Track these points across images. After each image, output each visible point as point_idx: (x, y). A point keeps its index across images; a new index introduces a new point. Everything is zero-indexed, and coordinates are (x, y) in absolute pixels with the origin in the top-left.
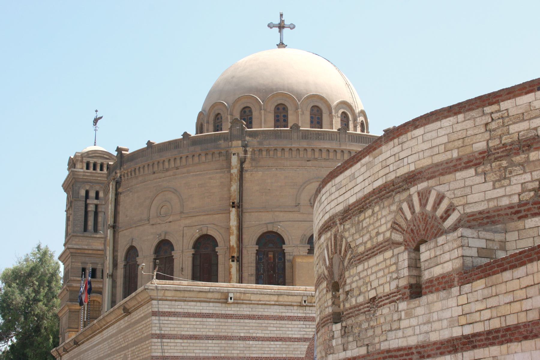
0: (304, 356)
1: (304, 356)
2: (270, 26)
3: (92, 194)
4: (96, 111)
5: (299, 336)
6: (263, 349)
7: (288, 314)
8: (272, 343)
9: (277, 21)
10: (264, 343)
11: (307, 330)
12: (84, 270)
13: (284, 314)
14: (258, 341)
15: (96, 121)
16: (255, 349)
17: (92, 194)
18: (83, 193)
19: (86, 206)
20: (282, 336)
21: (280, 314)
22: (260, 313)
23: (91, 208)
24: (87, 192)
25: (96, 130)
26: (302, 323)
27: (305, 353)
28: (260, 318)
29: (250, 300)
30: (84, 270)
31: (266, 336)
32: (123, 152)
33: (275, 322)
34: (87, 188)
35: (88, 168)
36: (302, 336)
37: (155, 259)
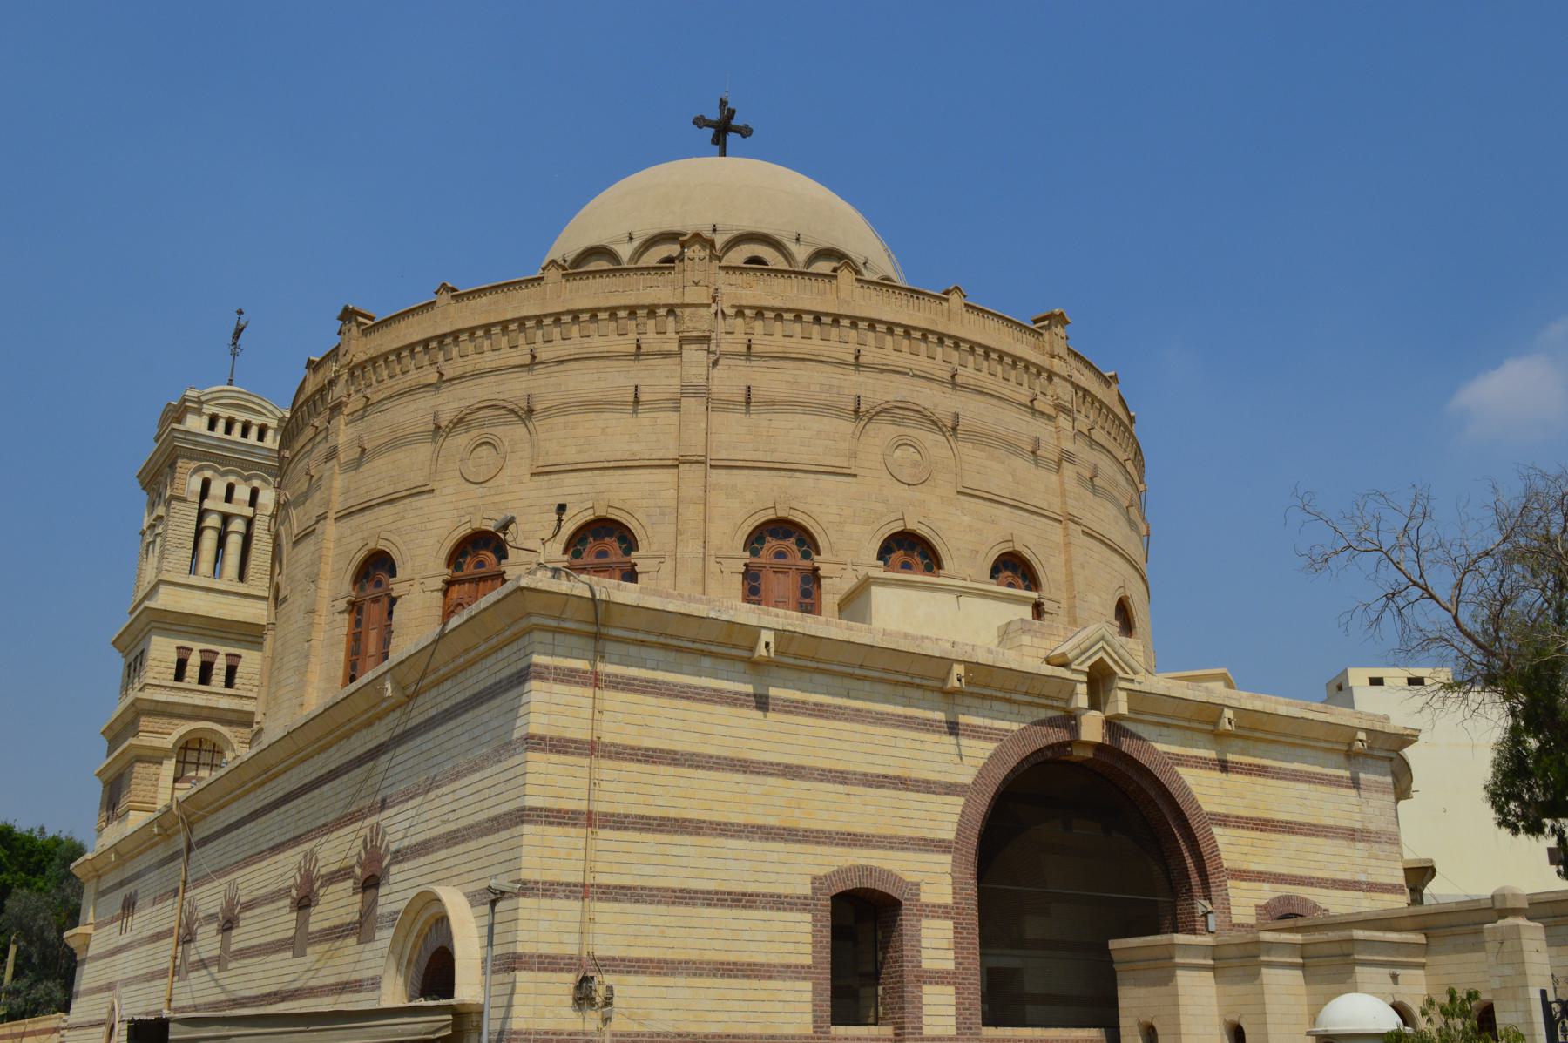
2: (700, 122)
3: (218, 488)
4: (240, 313)
9: (714, 115)
12: (181, 665)
15: (239, 332)
17: (218, 488)
18: (196, 484)
19: (202, 514)
23: (213, 521)
24: (206, 484)
25: (235, 355)
29: (812, 659)
30: (181, 665)
32: (360, 319)
34: (208, 474)
35: (212, 427)
37: (449, 584)
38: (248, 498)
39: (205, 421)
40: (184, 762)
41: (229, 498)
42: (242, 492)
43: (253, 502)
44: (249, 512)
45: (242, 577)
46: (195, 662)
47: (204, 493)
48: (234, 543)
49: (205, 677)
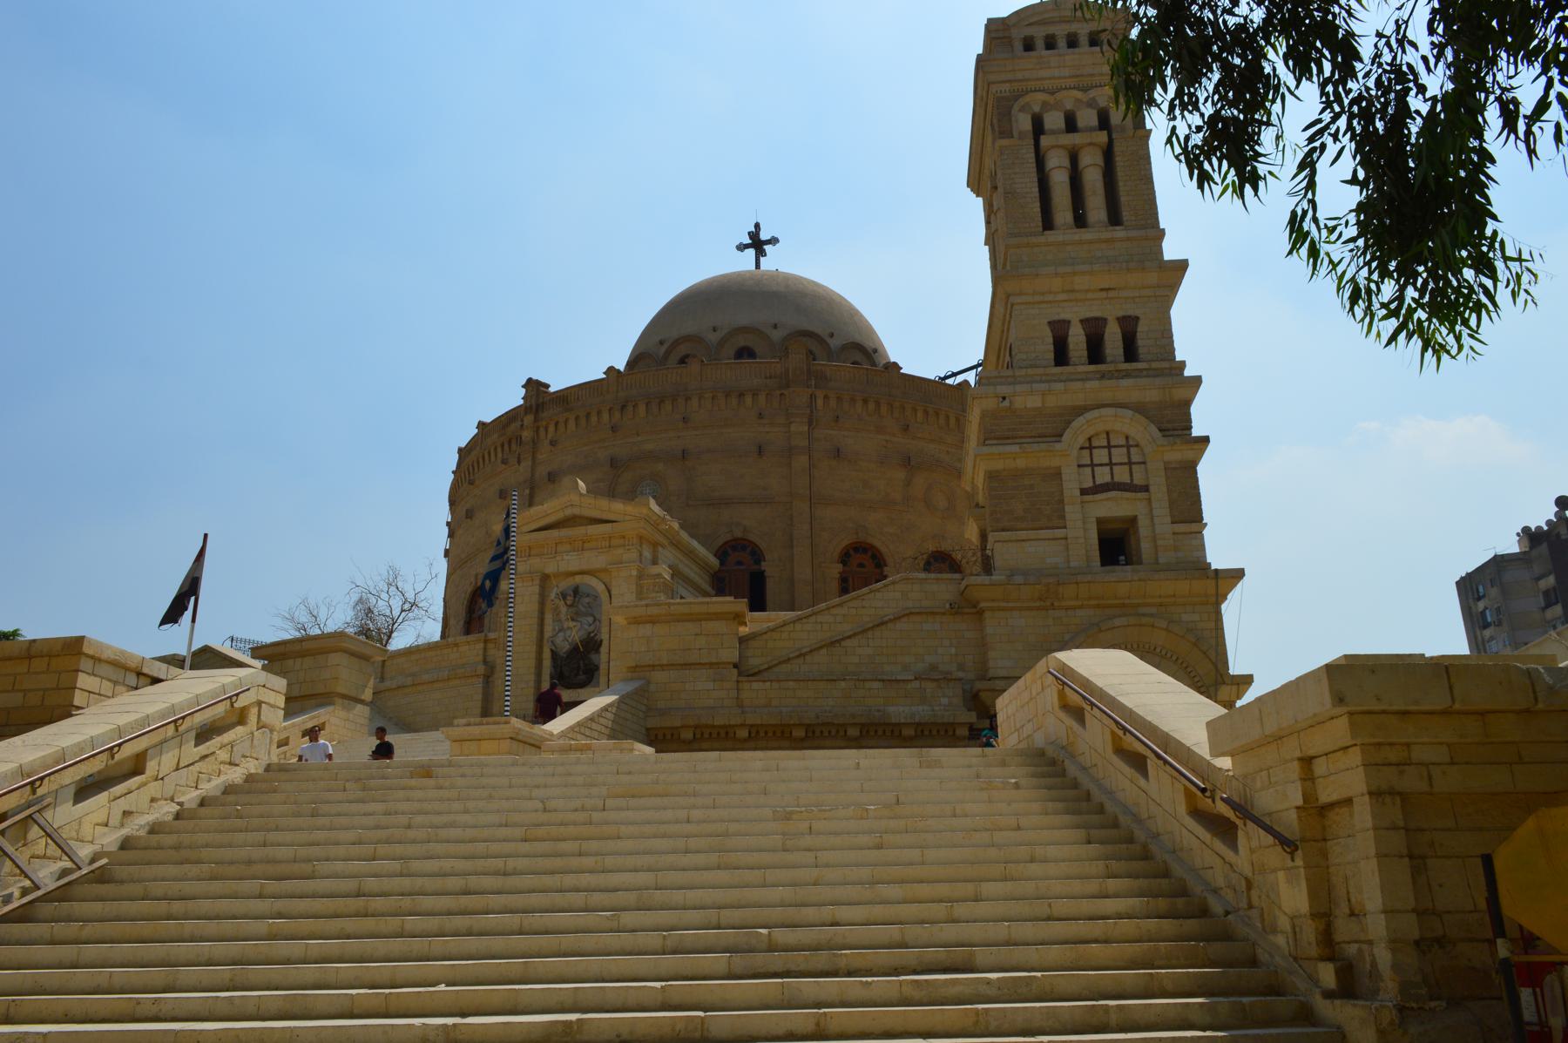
3: (1054, 120)
17: (1054, 120)
18: (1024, 123)
34: (1037, 109)
38: (1095, 122)
39: (1018, 46)
40: (1092, 465)
41: (1071, 125)
42: (1087, 118)
43: (1104, 122)
44: (1102, 137)
45: (1115, 218)
46: (1077, 340)
47: (1038, 128)
48: (1093, 178)
49: (1095, 353)
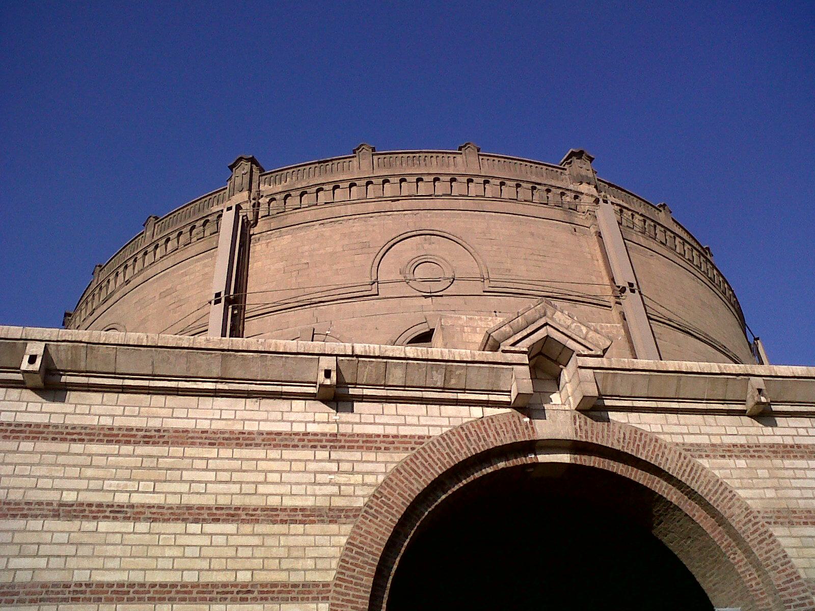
0: (330, 577)
1: (330, 577)
5: (309, 502)
6: (154, 551)
7: (266, 427)
8: (194, 528)
10: (158, 527)
11: (342, 479)
13: (251, 427)
14: (136, 519)
16: (118, 550)
20: (238, 501)
21: (238, 427)
22: (155, 423)
26: (322, 454)
27: (334, 564)
28: (150, 437)
31: (173, 500)
33: (213, 452)
36: (322, 502)
